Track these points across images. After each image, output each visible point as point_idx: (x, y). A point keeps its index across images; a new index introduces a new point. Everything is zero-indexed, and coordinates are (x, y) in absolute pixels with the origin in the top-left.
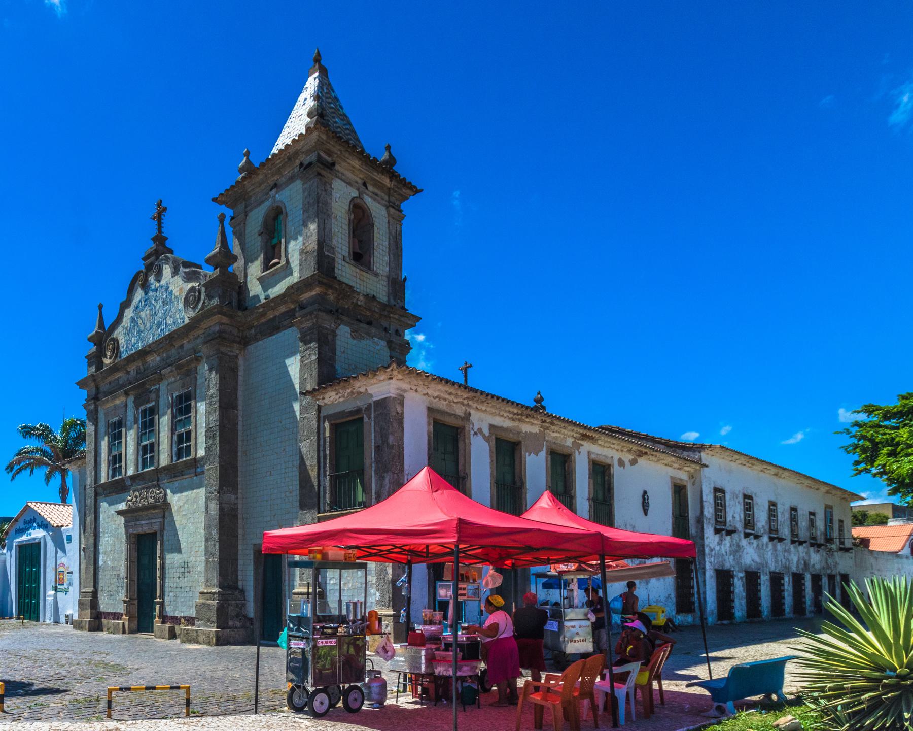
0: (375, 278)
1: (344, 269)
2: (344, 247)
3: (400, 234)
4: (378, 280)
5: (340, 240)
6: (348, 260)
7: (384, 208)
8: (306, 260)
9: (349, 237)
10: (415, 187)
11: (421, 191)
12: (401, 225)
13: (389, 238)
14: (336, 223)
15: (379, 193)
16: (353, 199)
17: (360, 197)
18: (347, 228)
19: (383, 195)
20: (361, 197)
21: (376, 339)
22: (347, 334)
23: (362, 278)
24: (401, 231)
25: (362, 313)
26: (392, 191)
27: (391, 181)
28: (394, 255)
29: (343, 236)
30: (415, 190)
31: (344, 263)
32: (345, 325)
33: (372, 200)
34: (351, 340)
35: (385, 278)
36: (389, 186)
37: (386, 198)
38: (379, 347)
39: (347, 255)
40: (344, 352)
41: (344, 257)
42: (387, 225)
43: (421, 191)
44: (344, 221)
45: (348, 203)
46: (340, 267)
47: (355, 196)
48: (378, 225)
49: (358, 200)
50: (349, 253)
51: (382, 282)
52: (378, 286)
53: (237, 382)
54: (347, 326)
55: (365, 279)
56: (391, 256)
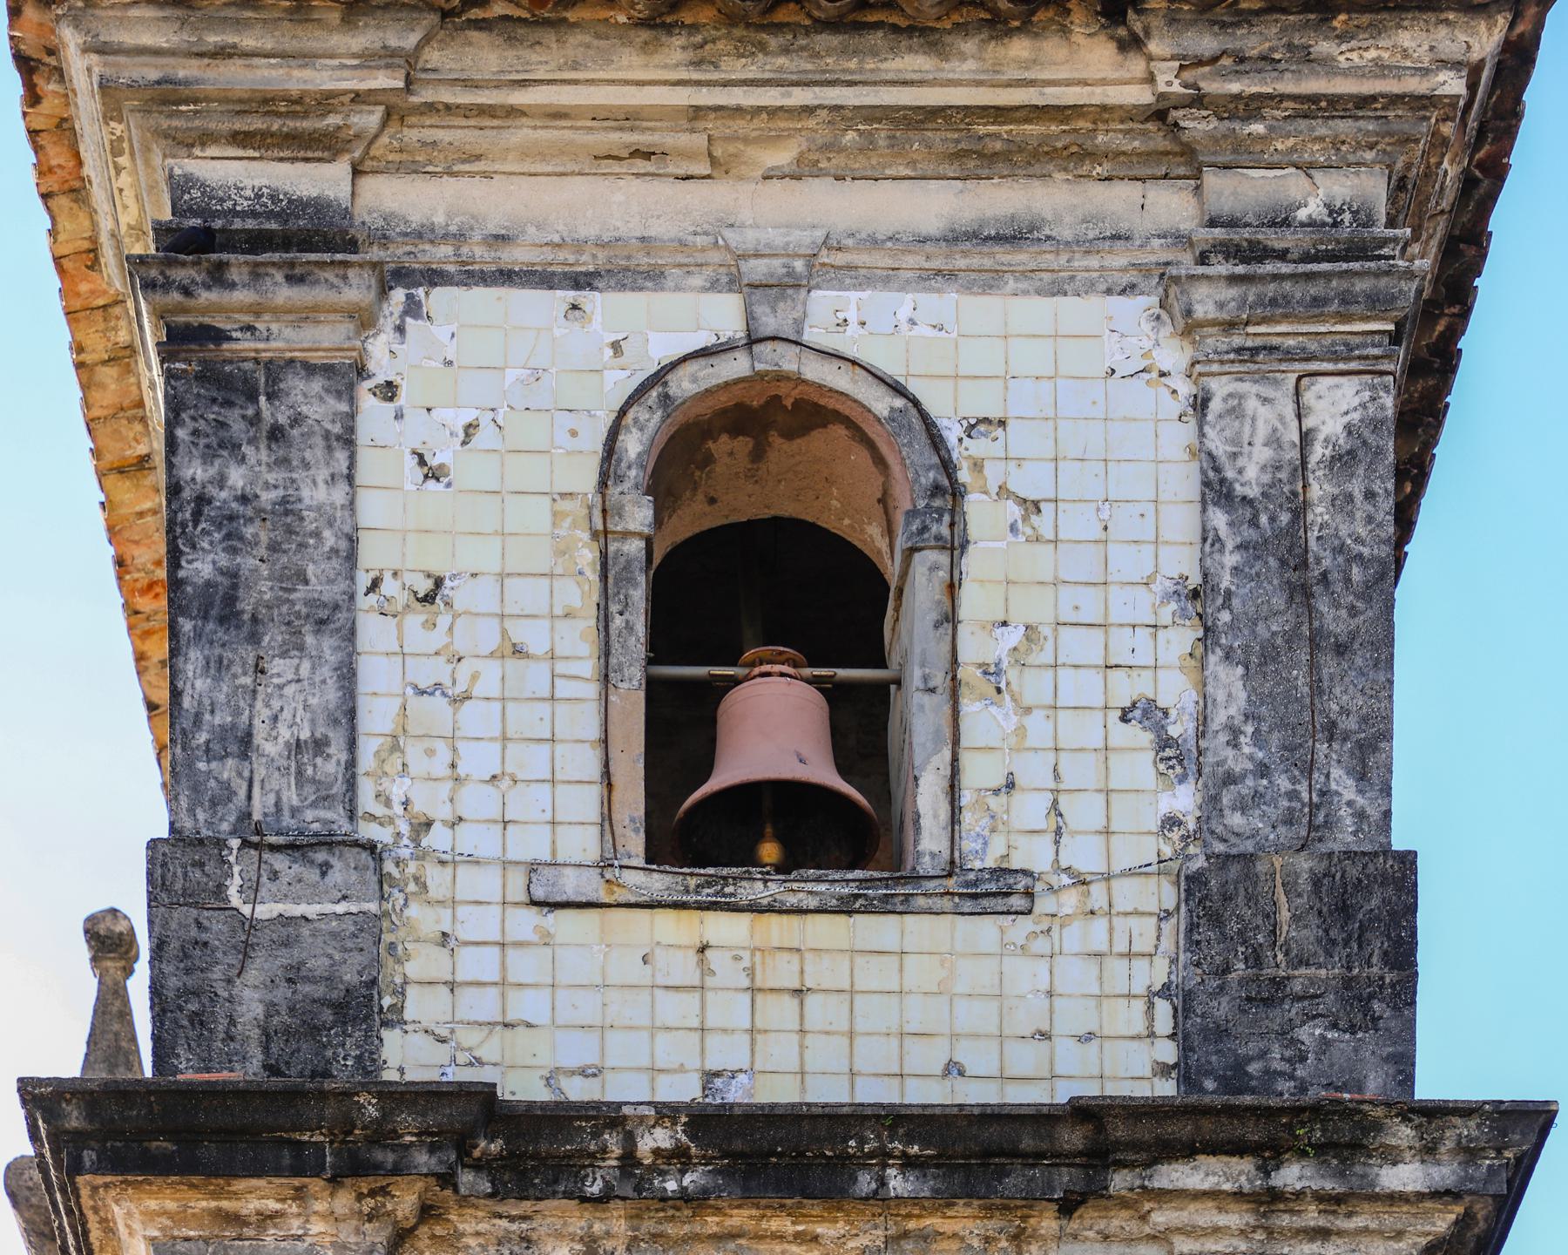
26: (1197, 126)
27: (1132, 44)
36: (1140, 96)
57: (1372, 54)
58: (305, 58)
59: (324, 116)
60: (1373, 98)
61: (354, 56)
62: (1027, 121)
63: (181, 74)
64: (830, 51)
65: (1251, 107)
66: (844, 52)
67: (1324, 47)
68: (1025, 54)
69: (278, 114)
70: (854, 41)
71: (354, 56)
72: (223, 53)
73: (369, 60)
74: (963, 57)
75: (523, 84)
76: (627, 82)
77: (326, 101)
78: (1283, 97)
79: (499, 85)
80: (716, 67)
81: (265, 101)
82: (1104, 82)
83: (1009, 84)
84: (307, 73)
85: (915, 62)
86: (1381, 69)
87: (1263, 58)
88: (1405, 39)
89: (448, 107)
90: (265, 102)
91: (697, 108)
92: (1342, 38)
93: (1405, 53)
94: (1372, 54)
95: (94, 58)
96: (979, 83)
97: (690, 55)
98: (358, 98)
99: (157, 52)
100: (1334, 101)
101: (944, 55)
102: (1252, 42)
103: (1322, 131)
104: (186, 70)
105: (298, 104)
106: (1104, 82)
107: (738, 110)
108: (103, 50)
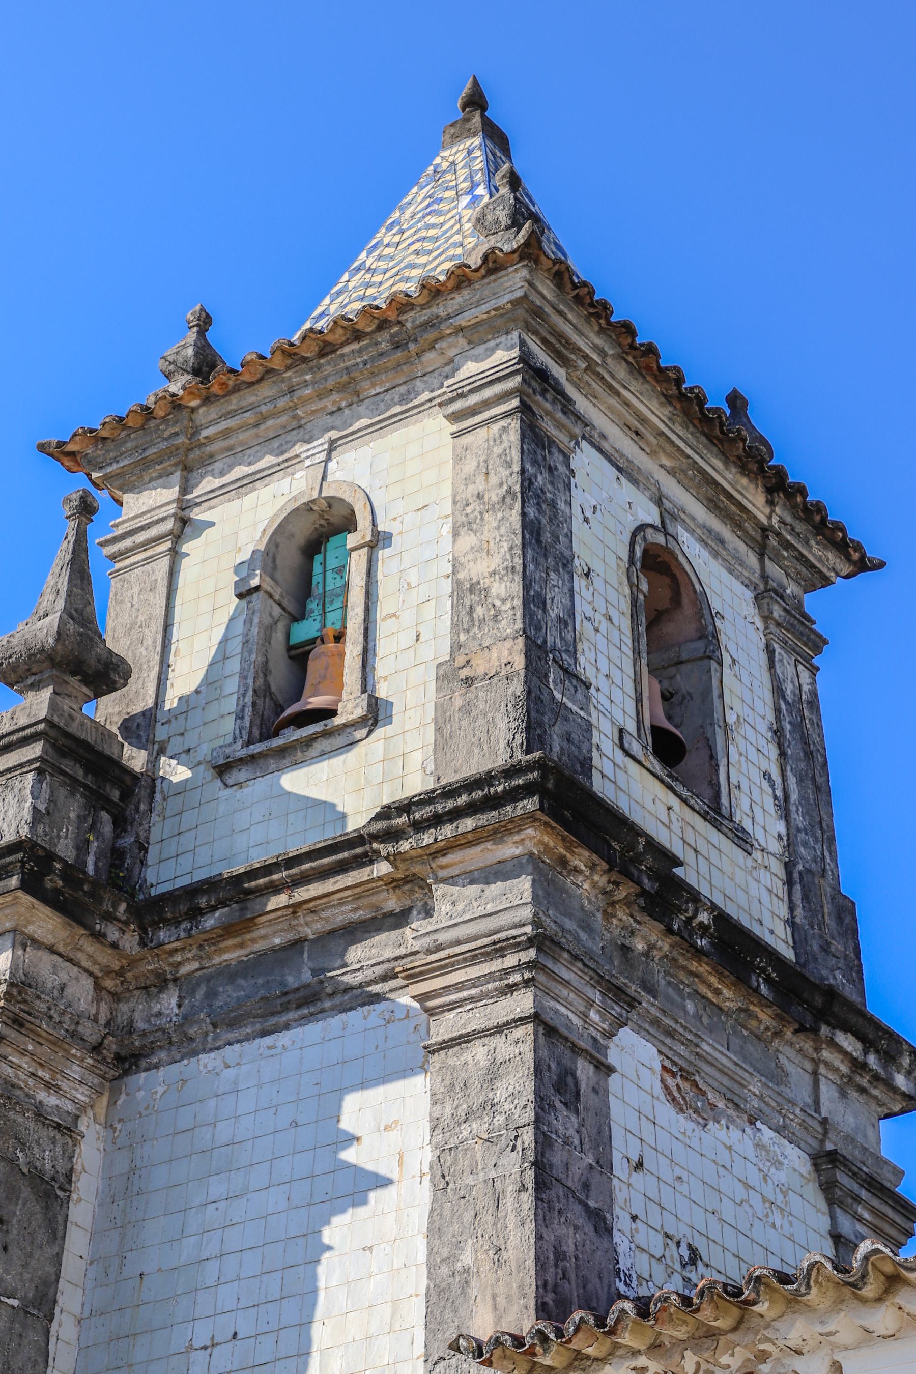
0: (739, 854)
1: (621, 778)
2: (617, 695)
3: (813, 703)
4: (750, 862)
5: (603, 663)
6: (636, 748)
7: (749, 595)
8: (466, 710)
9: (637, 652)
10: (858, 547)
11: (882, 565)
12: (814, 670)
13: (777, 711)
14: (587, 595)
15: (725, 532)
16: (642, 528)
17: (663, 529)
18: (625, 624)
19: (742, 547)
20: (670, 529)
21: (767, 1134)
22: (645, 1073)
23: (690, 839)
24: (814, 694)
25: (703, 990)
26: (773, 541)
27: (771, 503)
28: (800, 781)
29: (615, 653)
30: (856, 556)
31: (619, 756)
32: (639, 1029)
33: (705, 554)
34: (666, 1112)
35: (777, 868)
36: (764, 520)
37: (752, 559)
38: (781, 1176)
39: (631, 726)
40: (639, 1165)
41: (621, 731)
42: (763, 658)
43: (882, 565)
44: (613, 596)
45: (627, 540)
46: (608, 769)
47: (650, 521)
48: (732, 648)
49: (660, 539)
50: (639, 722)
51: (765, 878)
52: (753, 885)
53: (57, 1259)
54: (649, 1037)
55: (702, 846)
56: (792, 780)
57: (820, 553)
58: (581, 333)
59: (572, 353)
60: (816, 568)
61: (593, 344)
62: (733, 504)
63: (546, 310)
64: (702, 443)
65: (788, 546)
66: (705, 447)
67: (812, 542)
68: (745, 484)
69: (561, 343)
70: (710, 445)
71: (593, 344)
72: (560, 313)
73: (595, 348)
74: (731, 473)
75: (625, 388)
76: (650, 410)
77: (577, 350)
78: (795, 549)
79: (619, 382)
80: (674, 424)
81: (561, 336)
82: (758, 509)
83: (737, 490)
84: (577, 338)
85: (719, 464)
86: (820, 559)
87: (798, 534)
88: (830, 555)
89: (603, 378)
90: (560, 336)
91: (663, 433)
92: (817, 543)
93: (828, 560)
94: (820, 553)
95: (526, 285)
96: (730, 483)
97: (670, 415)
98: (586, 357)
99: (544, 298)
100: (807, 560)
101: (727, 468)
102: (800, 527)
103: (798, 567)
104: (548, 310)
105: (568, 343)
106: (758, 509)
107: (672, 442)
108: (531, 284)
